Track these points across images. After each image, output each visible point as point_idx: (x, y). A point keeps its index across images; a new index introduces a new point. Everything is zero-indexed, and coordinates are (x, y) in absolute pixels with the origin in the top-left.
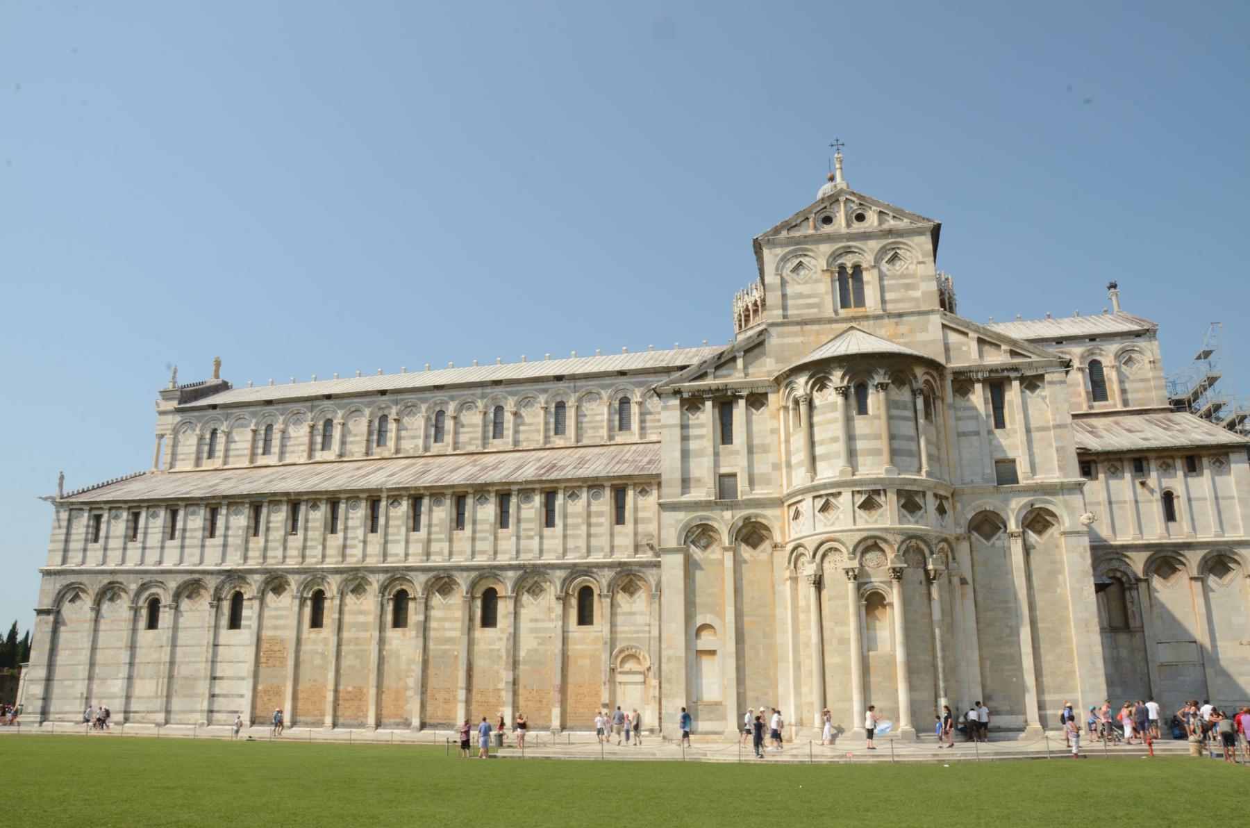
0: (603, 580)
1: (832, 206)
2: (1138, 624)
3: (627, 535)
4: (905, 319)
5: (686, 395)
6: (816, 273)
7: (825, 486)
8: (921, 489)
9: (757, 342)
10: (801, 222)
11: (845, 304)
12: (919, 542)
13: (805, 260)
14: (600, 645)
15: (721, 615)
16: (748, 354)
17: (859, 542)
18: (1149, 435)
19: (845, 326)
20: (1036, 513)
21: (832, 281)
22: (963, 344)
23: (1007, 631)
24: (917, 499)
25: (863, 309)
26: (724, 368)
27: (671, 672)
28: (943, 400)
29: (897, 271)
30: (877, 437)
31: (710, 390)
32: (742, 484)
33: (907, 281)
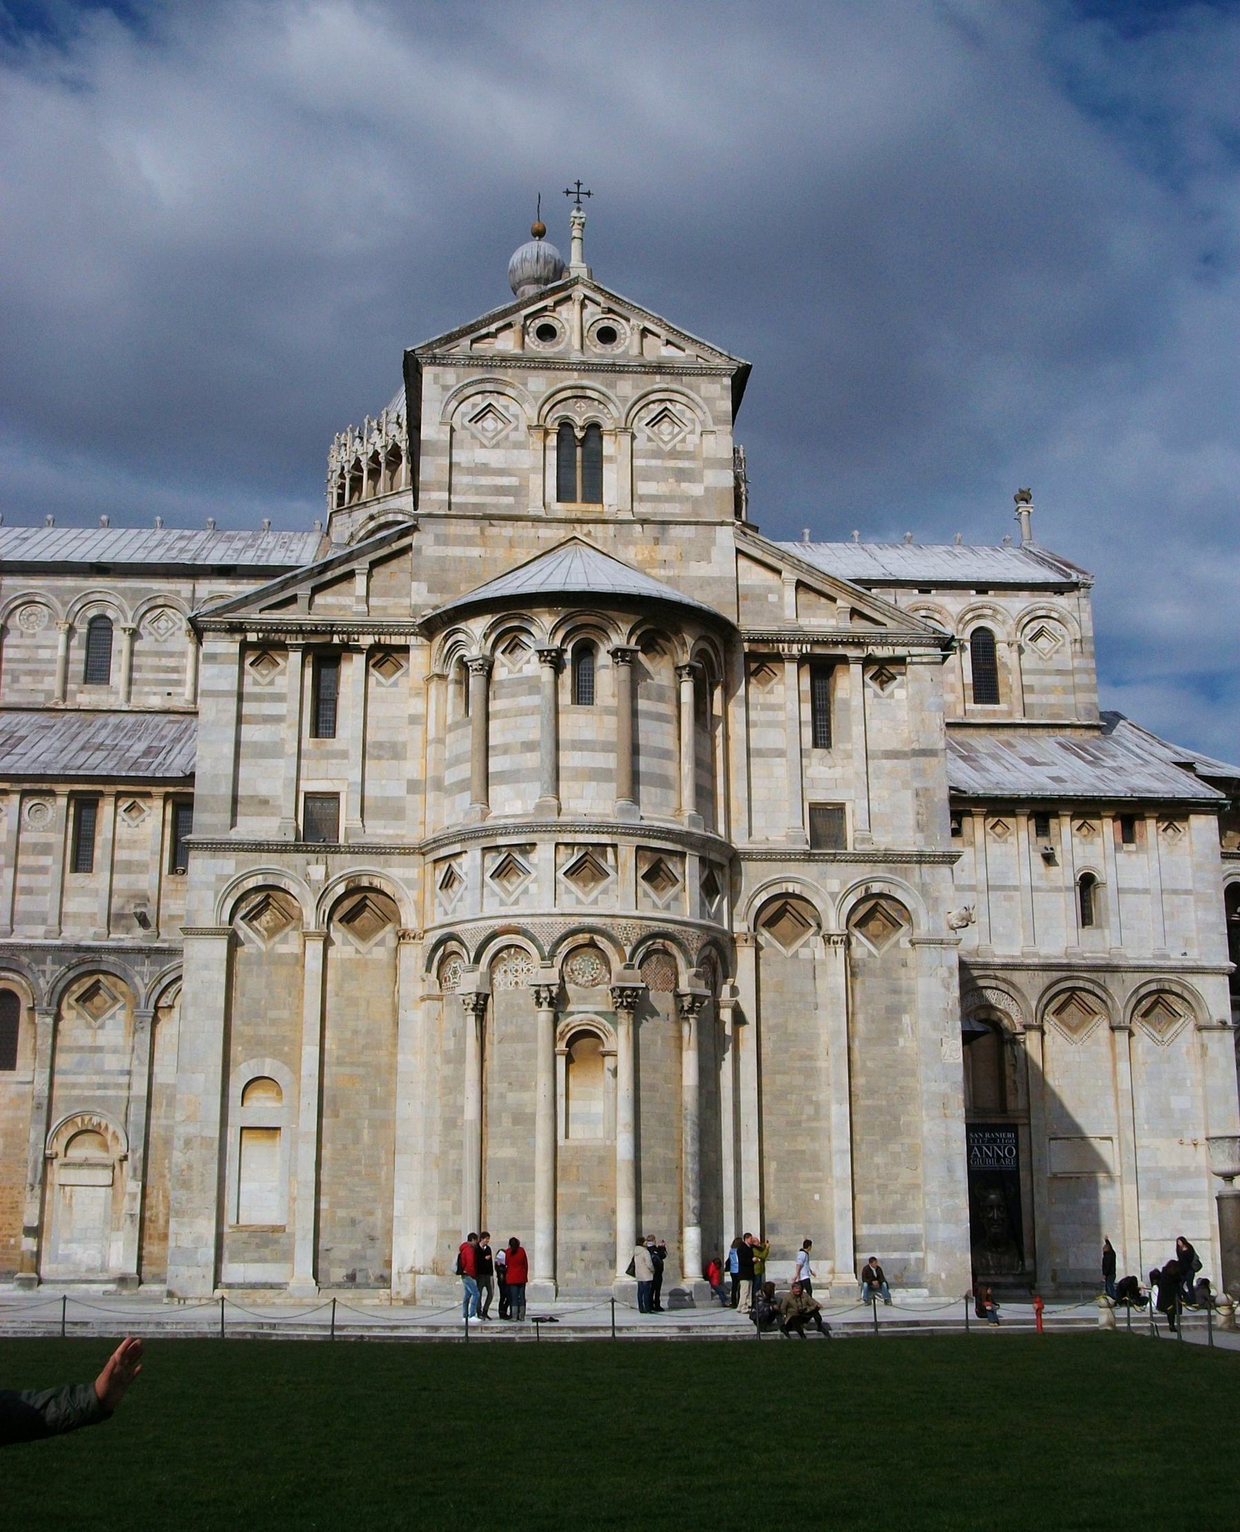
0: (42, 981)
2: (1021, 1104)
3: (95, 893)
4: (675, 531)
5: (252, 637)
6: (516, 429)
7: (505, 831)
10: (499, 330)
11: (564, 494)
12: (668, 943)
13: (499, 402)
14: (27, 1109)
15: (294, 1064)
17: (563, 938)
18: (1063, 774)
19: (561, 533)
20: (872, 902)
22: (770, 590)
23: (810, 1110)
24: (671, 867)
25: (598, 508)
26: (330, 590)
27: (190, 1167)
30: (606, 747)
32: (348, 817)
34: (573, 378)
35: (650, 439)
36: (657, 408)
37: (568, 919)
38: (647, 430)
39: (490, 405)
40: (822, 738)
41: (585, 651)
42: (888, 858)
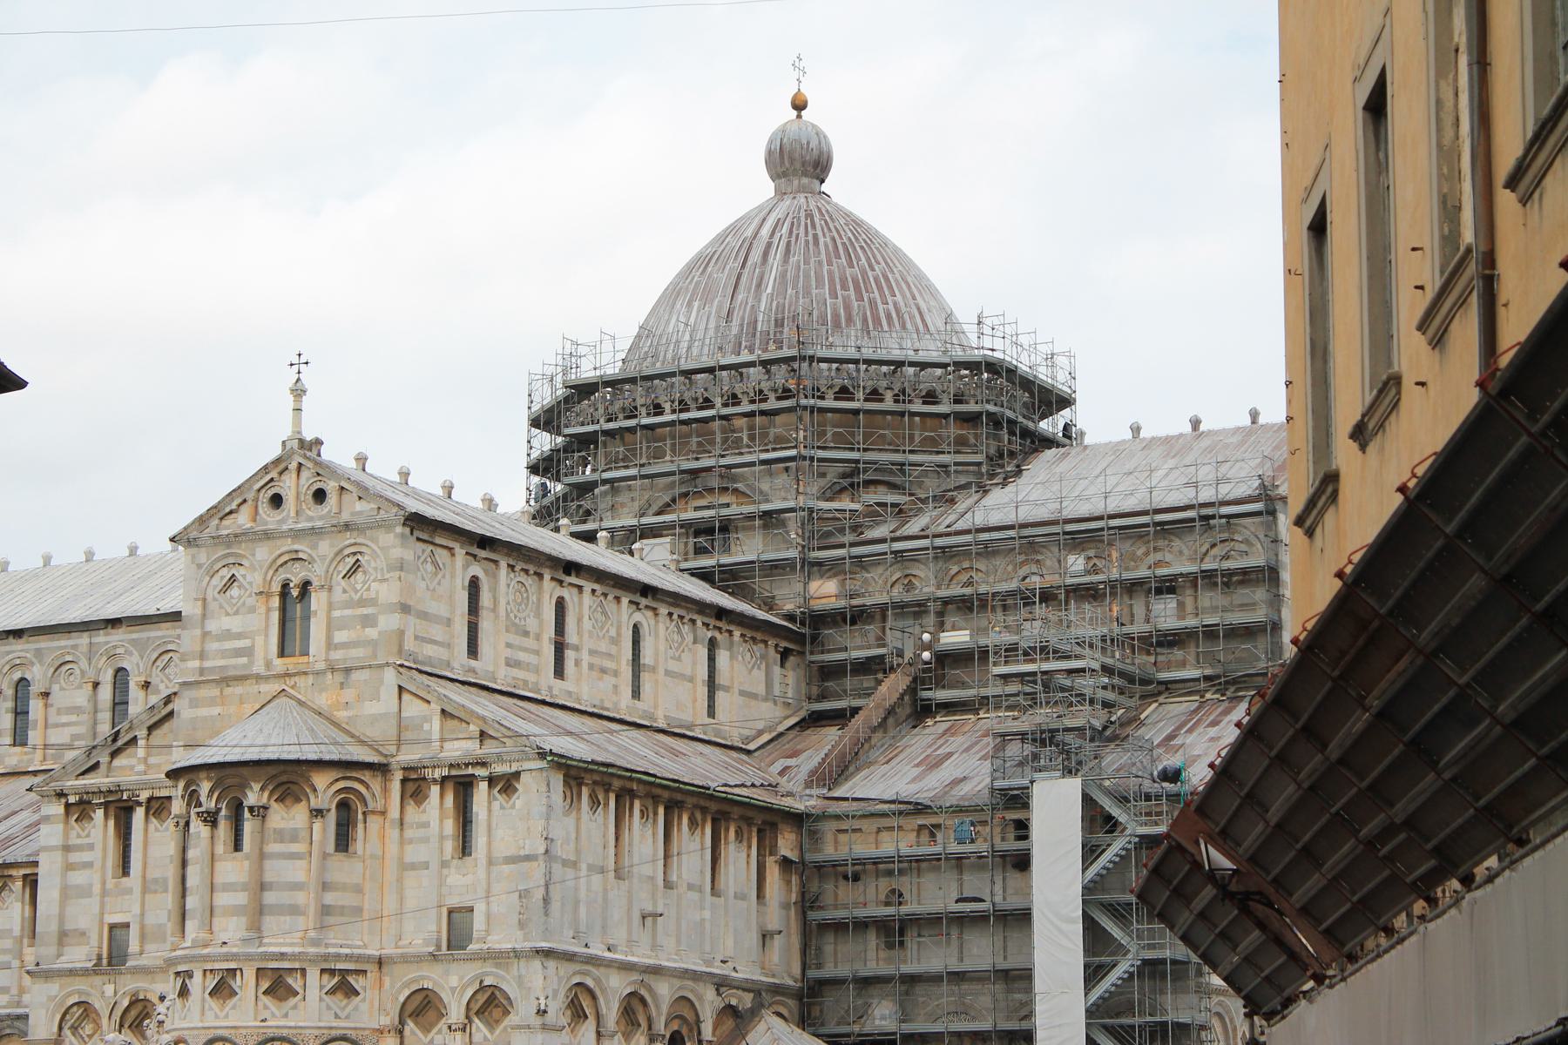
1: (283, 477)
4: (355, 676)
5: (72, 799)
6: (250, 596)
8: (297, 965)
9: (164, 712)
10: (239, 505)
16: (156, 733)
19: (275, 687)
20: (489, 993)
21: (269, 610)
24: (290, 981)
28: (383, 813)
29: (356, 591)
31: (101, 792)
33: (366, 611)
34: (288, 545)
35: (345, 591)
36: (351, 560)
37: (207, 1032)
38: (343, 583)
39: (233, 575)
40: (465, 848)
41: (237, 809)
42: (498, 957)
